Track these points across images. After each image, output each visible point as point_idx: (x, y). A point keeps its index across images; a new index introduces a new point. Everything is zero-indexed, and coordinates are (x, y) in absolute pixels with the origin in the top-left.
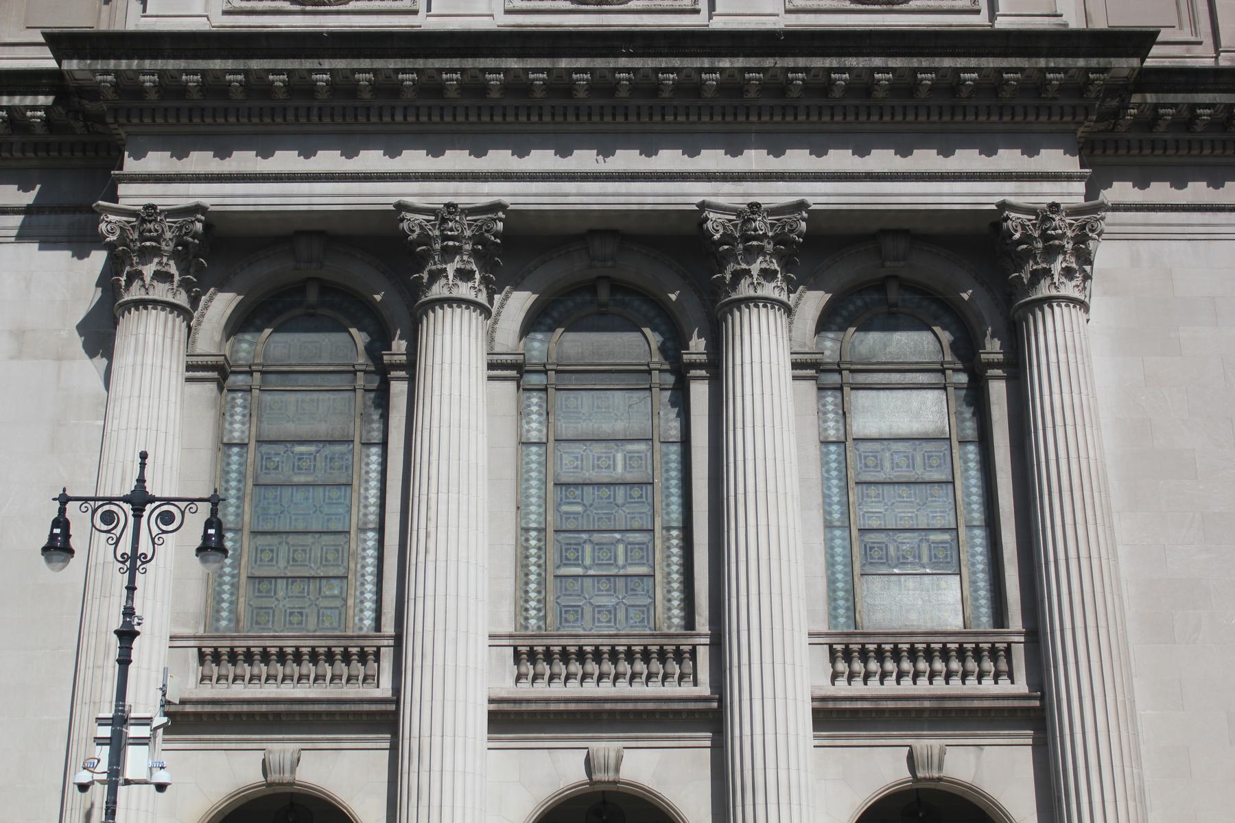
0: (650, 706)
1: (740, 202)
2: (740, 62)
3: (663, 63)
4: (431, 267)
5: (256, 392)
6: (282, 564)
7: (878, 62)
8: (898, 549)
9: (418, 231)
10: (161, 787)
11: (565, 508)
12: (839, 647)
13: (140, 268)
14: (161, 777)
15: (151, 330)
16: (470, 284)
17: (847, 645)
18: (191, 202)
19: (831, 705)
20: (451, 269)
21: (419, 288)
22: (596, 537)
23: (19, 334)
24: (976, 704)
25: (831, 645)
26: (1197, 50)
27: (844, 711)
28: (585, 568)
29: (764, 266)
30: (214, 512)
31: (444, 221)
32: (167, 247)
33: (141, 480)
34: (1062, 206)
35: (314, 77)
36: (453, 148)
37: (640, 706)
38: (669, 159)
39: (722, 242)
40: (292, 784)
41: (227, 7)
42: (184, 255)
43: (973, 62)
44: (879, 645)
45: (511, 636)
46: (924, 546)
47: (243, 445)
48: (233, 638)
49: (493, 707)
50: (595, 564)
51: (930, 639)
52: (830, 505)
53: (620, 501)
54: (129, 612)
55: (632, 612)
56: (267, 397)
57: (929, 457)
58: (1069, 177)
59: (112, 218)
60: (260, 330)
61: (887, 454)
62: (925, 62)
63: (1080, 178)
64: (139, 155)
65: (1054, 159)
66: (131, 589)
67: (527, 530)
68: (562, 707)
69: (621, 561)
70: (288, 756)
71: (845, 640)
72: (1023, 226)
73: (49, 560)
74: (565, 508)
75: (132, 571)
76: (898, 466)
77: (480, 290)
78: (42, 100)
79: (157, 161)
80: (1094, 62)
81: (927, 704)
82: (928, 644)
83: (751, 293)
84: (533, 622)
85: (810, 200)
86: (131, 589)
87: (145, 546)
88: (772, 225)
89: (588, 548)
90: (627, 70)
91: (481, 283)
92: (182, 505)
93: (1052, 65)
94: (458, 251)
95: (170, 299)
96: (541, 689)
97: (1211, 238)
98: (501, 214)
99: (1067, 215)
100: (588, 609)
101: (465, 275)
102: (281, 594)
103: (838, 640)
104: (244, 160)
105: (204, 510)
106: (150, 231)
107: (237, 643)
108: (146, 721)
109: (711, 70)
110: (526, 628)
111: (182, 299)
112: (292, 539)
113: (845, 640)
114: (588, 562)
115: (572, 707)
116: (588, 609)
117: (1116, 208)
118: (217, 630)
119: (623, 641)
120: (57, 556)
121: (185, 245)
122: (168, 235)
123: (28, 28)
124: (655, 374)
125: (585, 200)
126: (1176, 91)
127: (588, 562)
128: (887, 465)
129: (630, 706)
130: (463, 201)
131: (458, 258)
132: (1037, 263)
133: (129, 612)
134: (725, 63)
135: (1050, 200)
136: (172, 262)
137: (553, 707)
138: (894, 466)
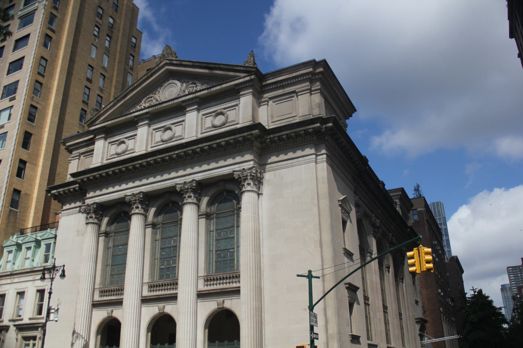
0: (168, 296)
1: (182, 182)
2: (179, 151)
3: (165, 155)
4: (242, 184)
5: (113, 237)
6: (116, 271)
7: (205, 144)
8: (223, 254)
9: (238, 176)
10: (56, 321)
11: (162, 253)
12: (206, 279)
13: (244, 183)
14: (56, 319)
15: (89, 228)
16: (250, 186)
17: (207, 278)
18: (93, 202)
19: (200, 293)
20: (134, 207)
21: (241, 189)
22: (167, 259)
23: (78, 231)
24: (229, 290)
25: (204, 279)
26: (296, 118)
27: (152, 299)
28: (165, 266)
29: (189, 195)
30: (64, 268)
31: (243, 172)
32: (92, 211)
33: (54, 264)
34: (245, 169)
35: (188, 152)
36: (220, 161)
37: (166, 296)
38: (166, 176)
39: (238, 179)
40: (223, 307)
41: (107, 159)
42: (194, 191)
43: (223, 140)
44: (213, 278)
45: (147, 283)
46: (229, 253)
47: (159, 240)
48: (104, 288)
49: (198, 293)
50: (167, 265)
51: (223, 275)
52: (210, 246)
53: (172, 250)
54: (51, 289)
55: (173, 275)
56: (116, 237)
57: (231, 231)
58: (249, 161)
59: (83, 207)
60: (161, 215)
61: (222, 232)
62: (214, 142)
63: (252, 160)
64: (89, 194)
65: (248, 157)
66: (51, 284)
67: (155, 259)
68: (153, 297)
69: (171, 264)
70: (162, 307)
71: (207, 277)
72: (239, 175)
73: (61, 278)
74: (162, 253)
75: (52, 281)
76: (225, 235)
77: (253, 187)
78: (78, 185)
79: (91, 194)
80: (248, 133)
81: (219, 291)
82: (223, 276)
83: (245, 190)
84: (155, 279)
85: (195, 179)
86: (51, 284)
87: (54, 277)
88: (190, 185)
89: (166, 262)
90: (159, 158)
91: (253, 185)
92: (59, 267)
93: (239, 136)
94: (247, 179)
95: (93, 221)
96: (212, 287)
97: (292, 166)
98: (195, 182)
99: (248, 170)
100: (165, 275)
101: (137, 208)
102: (115, 277)
103: (205, 277)
104: (105, 191)
105: (62, 267)
106: (244, 174)
107: (105, 289)
108: (54, 309)
109: (174, 154)
110: (154, 280)
111: (96, 221)
112: (118, 266)
113: (207, 277)
114: (166, 265)
115: (155, 297)
116: (165, 275)
117: (311, 155)
118: (105, 286)
119: (166, 282)
120: (62, 277)
121: (141, 201)
122: (92, 209)
123: (278, 117)
124: (235, 211)
125: (158, 187)
126: (277, 133)
127: (166, 265)
128: (222, 235)
129: (164, 296)
130: (135, 192)
131: (136, 204)
132: (248, 181)
133: (51, 289)
134: (176, 152)
135: (242, 168)
136: (251, 181)
137: (151, 297)
138: (224, 235)
